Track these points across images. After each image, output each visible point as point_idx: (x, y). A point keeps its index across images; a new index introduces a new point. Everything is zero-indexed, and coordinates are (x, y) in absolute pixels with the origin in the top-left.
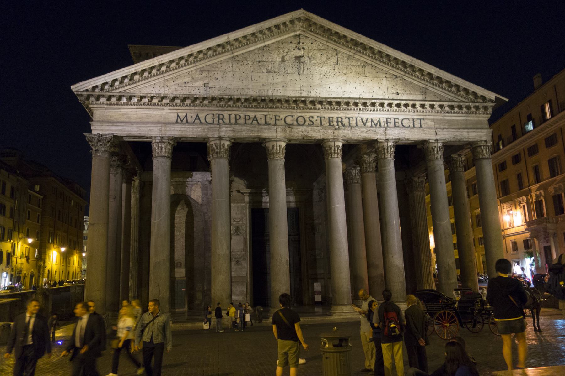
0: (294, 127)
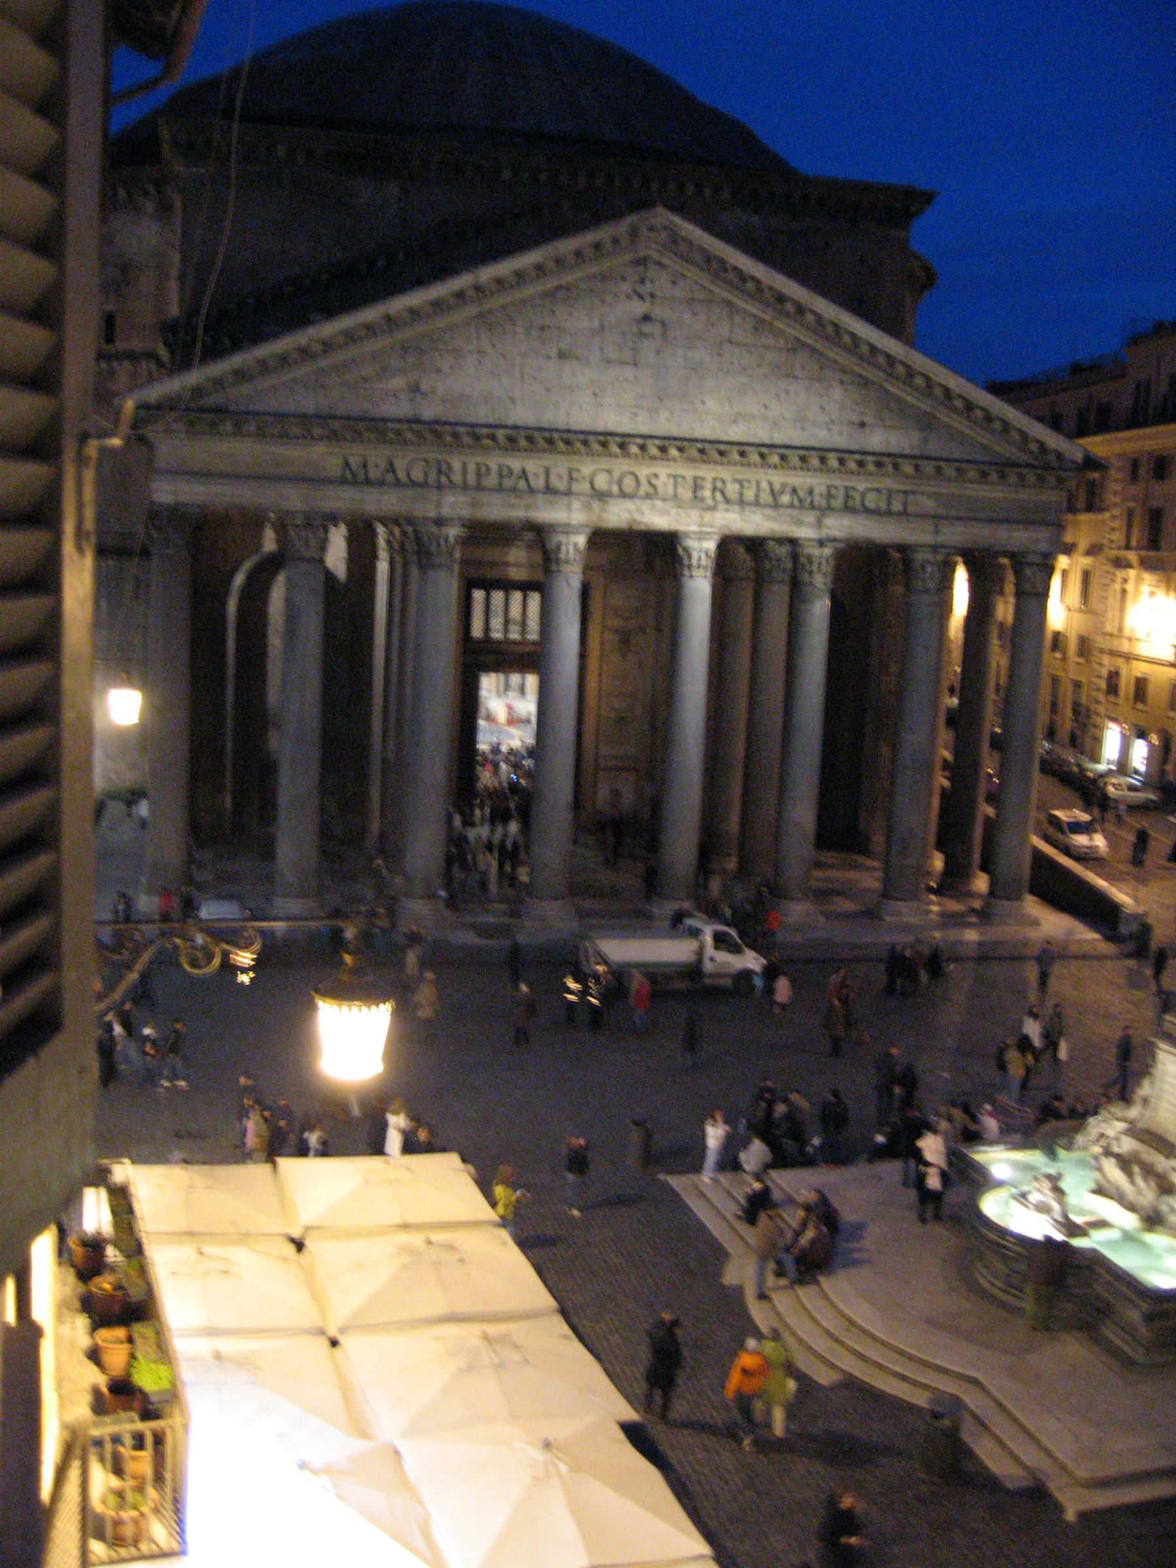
0: (612, 501)
